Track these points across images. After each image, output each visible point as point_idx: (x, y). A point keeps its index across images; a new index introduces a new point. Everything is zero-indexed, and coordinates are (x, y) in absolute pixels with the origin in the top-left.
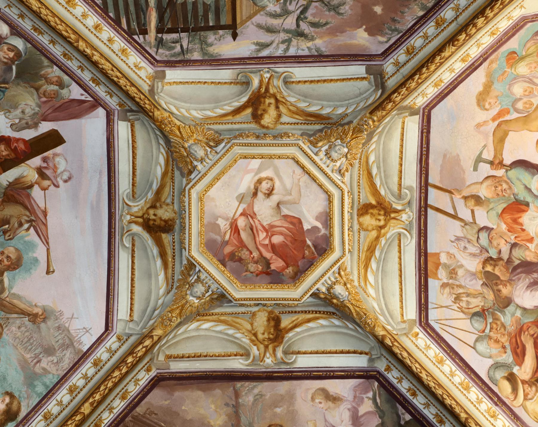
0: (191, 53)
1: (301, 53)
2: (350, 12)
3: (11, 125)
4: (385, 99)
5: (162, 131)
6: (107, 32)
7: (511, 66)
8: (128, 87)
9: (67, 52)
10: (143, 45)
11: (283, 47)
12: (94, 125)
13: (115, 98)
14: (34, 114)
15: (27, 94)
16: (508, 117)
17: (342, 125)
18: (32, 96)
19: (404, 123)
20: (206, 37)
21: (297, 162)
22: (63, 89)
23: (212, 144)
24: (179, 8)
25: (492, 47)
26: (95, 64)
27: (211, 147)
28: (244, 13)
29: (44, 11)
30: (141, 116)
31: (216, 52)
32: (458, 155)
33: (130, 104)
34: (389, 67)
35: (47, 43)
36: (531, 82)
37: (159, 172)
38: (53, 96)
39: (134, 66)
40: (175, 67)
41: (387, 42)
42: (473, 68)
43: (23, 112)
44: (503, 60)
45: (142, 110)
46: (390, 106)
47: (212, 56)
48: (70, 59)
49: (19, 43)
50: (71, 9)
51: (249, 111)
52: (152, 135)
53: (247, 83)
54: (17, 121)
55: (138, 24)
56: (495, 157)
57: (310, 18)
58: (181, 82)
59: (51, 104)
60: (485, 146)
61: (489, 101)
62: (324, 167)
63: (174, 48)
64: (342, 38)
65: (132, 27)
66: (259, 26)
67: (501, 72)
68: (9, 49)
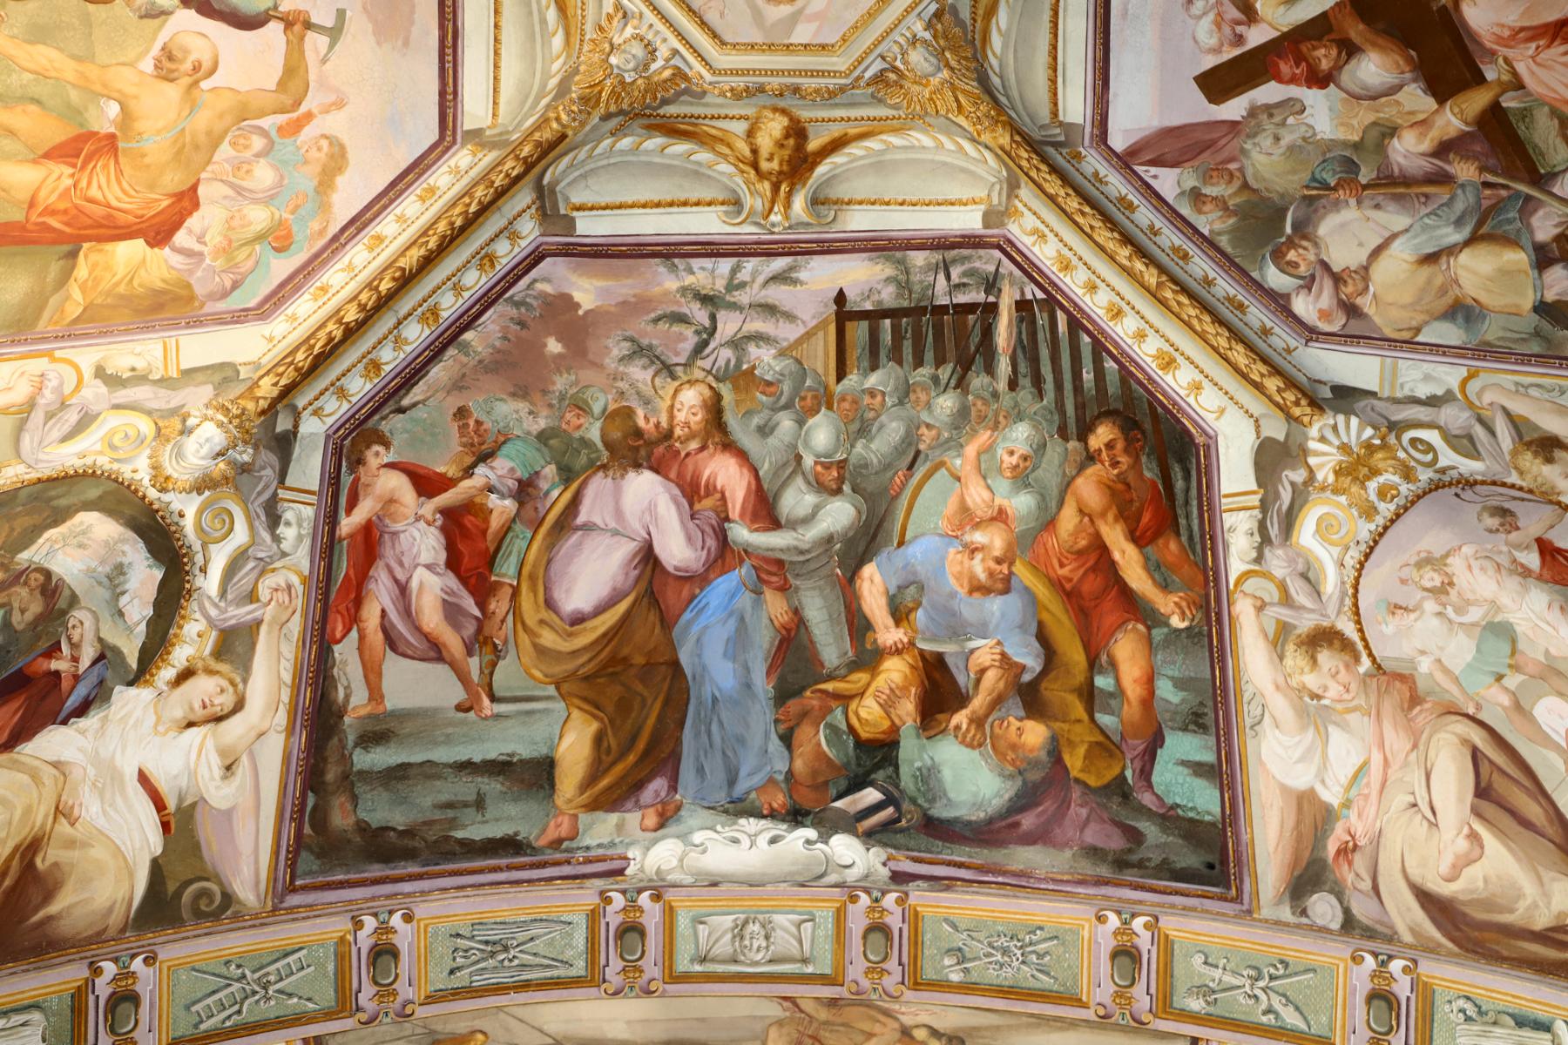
0: (929, 264)
1: (707, 263)
2: (610, 342)
3: (1303, 111)
4: (536, 164)
5: (992, 99)
6: (1097, 305)
7: (281, 223)
8: (1062, 192)
9: (1181, 263)
10: (1026, 279)
11: (744, 275)
12: (1132, 118)
13: (1089, 171)
14: (1255, 135)
15: (1266, 175)
16: (281, 119)
17: (621, 112)
18: (1255, 176)
19: (494, 115)
20: (899, 296)
21: (715, 35)
22: (1194, 188)
23: (892, 76)
24: (951, 353)
25: (325, 262)
26: (1127, 239)
27: (895, 69)
28: (821, 343)
29: (1222, 342)
30: (1036, 135)
31: (880, 267)
32: (379, 43)
33: (1059, 159)
34: (530, 231)
35: (1220, 281)
36: (239, 190)
37: (1003, 17)
38: (1215, 174)
39: (1047, 238)
40: (963, 236)
41: (535, 281)
42: (359, 222)
43: (1277, 139)
44: (298, 237)
45: (1035, 147)
46: (526, 150)
47: (887, 259)
48: (1176, 250)
49: (1275, 278)
50: (1166, 347)
51: (813, 145)
52: (1015, 93)
53: (816, 202)
54: (1291, 120)
55: (1033, 322)
56: (302, 38)
57: (689, 332)
58: (952, 204)
59: (1219, 157)
60: (324, 61)
61: (322, 155)
62: (659, 26)
63: (965, 274)
64: (624, 291)
65: (1045, 315)
66: (790, 317)
67: (301, 211)
68: (1296, 265)
